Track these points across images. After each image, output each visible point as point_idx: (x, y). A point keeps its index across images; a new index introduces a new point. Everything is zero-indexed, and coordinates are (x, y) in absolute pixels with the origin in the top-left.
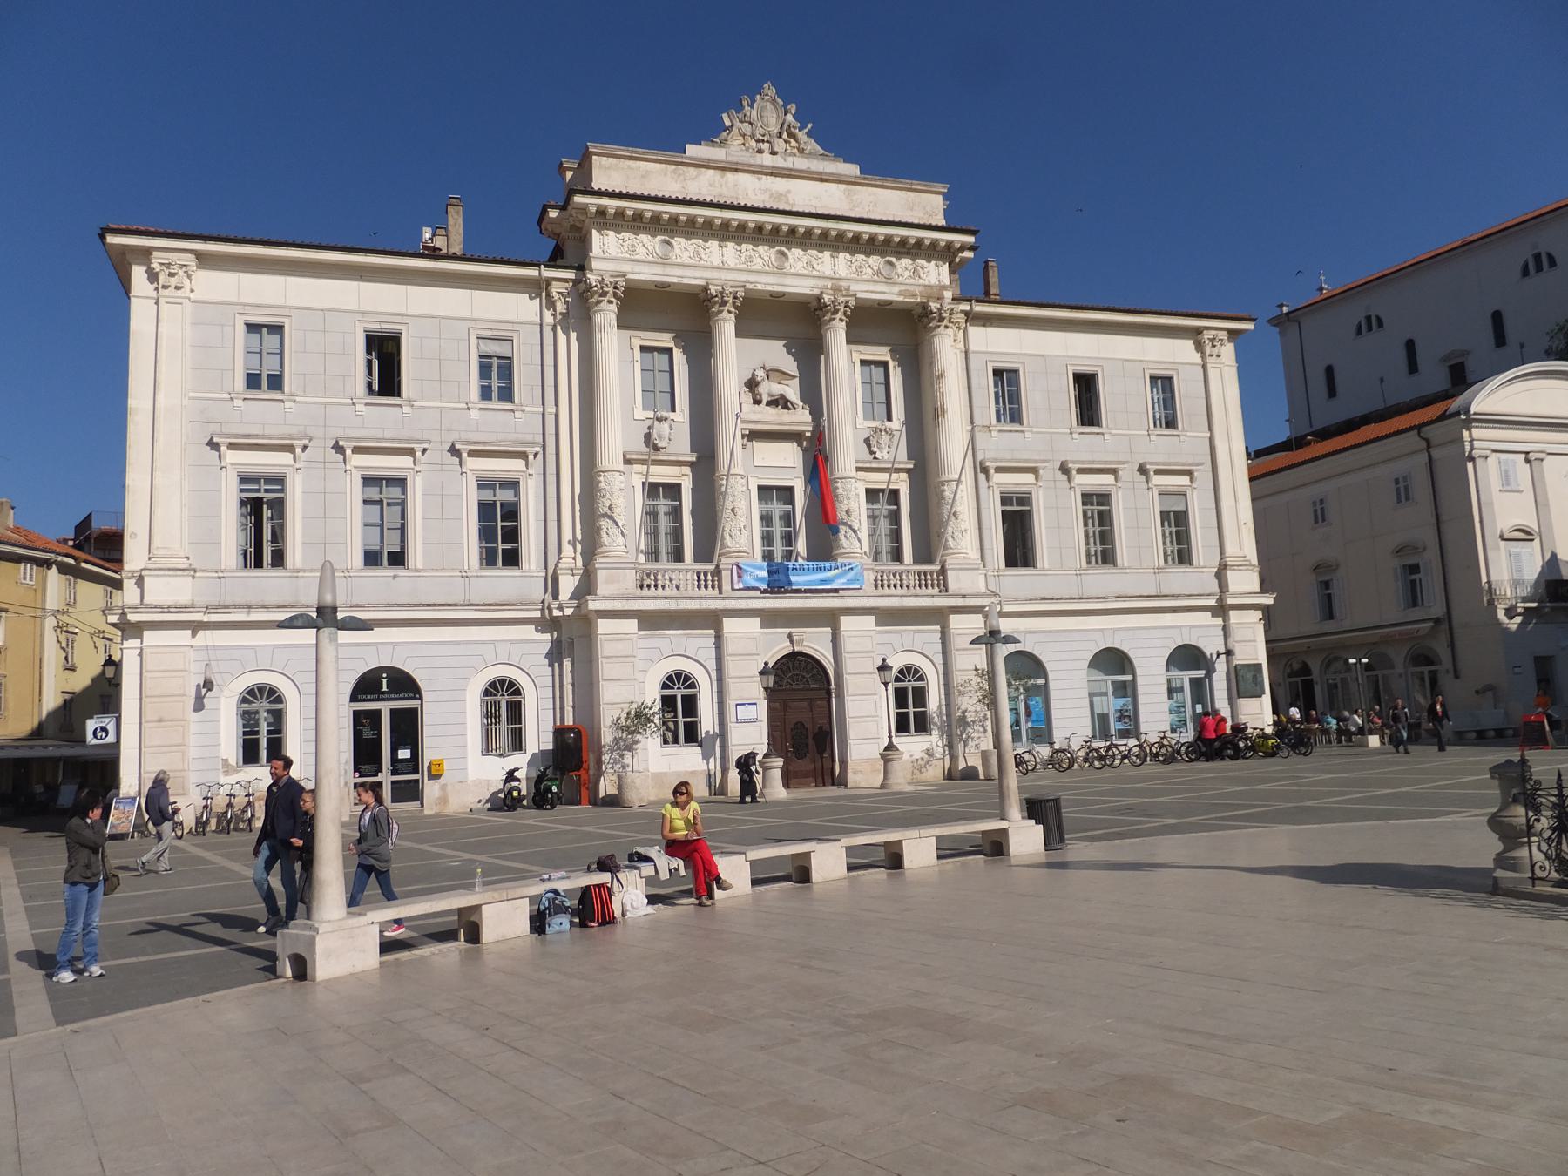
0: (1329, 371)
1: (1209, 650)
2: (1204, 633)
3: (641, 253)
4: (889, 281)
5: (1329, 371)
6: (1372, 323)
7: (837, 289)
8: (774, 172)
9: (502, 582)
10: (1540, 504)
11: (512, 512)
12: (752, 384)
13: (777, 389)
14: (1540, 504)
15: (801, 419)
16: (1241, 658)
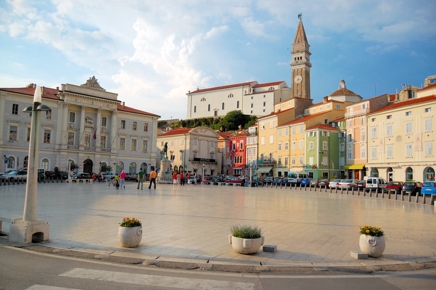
0: (195, 107)
1: (148, 164)
2: (147, 161)
3: (73, 100)
4: (108, 107)
5: (195, 107)
6: (204, 99)
7: (100, 108)
8: (93, 89)
9: (47, 145)
10: (199, 147)
11: (49, 135)
12: (86, 119)
13: (90, 121)
14: (199, 147)
15: (93, 125)
16: (152, 165)
